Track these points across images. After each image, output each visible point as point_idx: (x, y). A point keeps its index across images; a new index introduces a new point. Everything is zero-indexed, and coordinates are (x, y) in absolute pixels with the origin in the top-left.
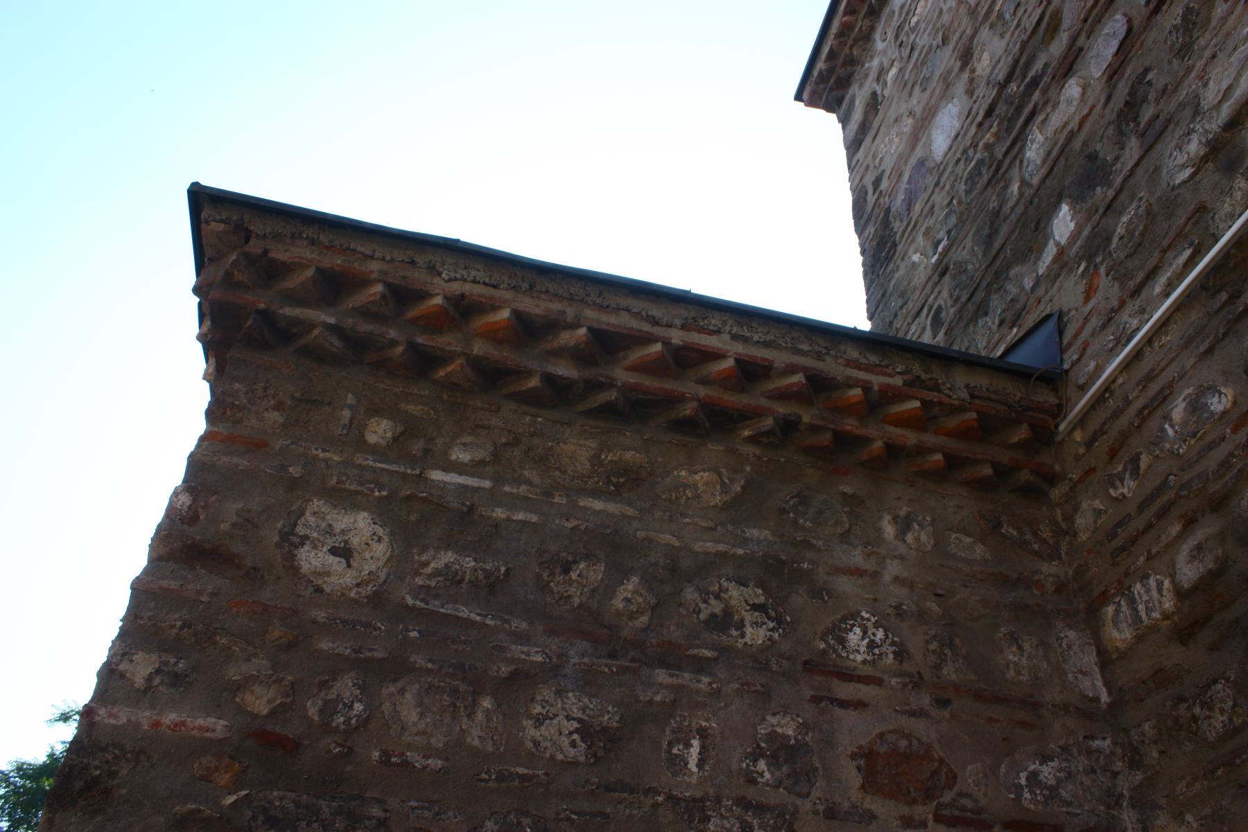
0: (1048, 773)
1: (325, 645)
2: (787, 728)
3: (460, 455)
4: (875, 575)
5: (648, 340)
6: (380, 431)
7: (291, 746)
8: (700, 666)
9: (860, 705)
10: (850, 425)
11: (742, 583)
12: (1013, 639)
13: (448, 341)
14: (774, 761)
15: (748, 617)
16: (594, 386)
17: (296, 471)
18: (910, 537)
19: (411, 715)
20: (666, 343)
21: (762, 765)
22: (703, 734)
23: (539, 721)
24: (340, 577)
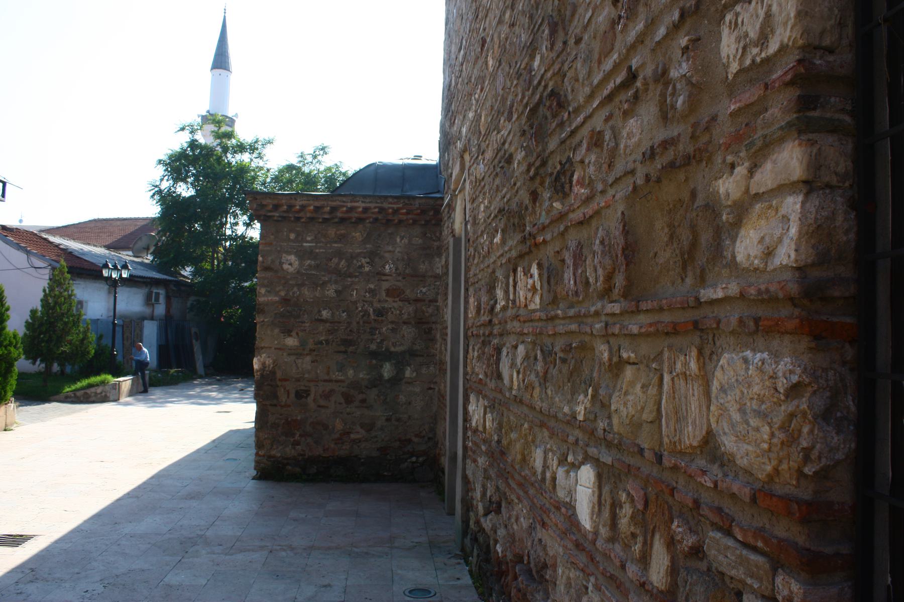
0: (424, 290)
1: (291, 282)
2: (372, 286)
3: (309, 239)
4: (394, 252)
5: (343, 206)
6: (292, 236)
7: (289, 300)
8: (356, 277)
9: (387, 280)
10: (390, 217)
11: (365, 258)
12: (423, 262)
13: (301, 215)
14: (369, 293)
15: (366, 265)
16: (333, 218)
17: (279, 249)
18: (403, 241)
19: (306, 293)
20: (347, 207)
21: (367, 294)
22: (356, 289)
23: (328, 291)
24: (291, 269)
